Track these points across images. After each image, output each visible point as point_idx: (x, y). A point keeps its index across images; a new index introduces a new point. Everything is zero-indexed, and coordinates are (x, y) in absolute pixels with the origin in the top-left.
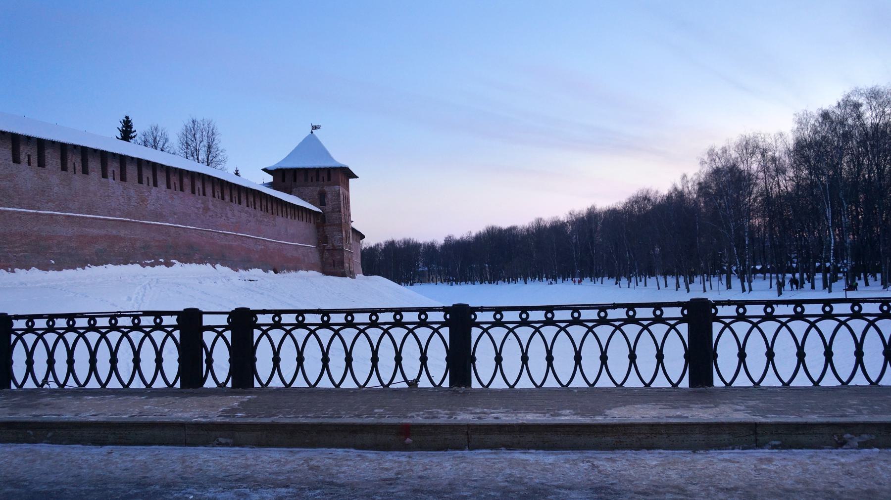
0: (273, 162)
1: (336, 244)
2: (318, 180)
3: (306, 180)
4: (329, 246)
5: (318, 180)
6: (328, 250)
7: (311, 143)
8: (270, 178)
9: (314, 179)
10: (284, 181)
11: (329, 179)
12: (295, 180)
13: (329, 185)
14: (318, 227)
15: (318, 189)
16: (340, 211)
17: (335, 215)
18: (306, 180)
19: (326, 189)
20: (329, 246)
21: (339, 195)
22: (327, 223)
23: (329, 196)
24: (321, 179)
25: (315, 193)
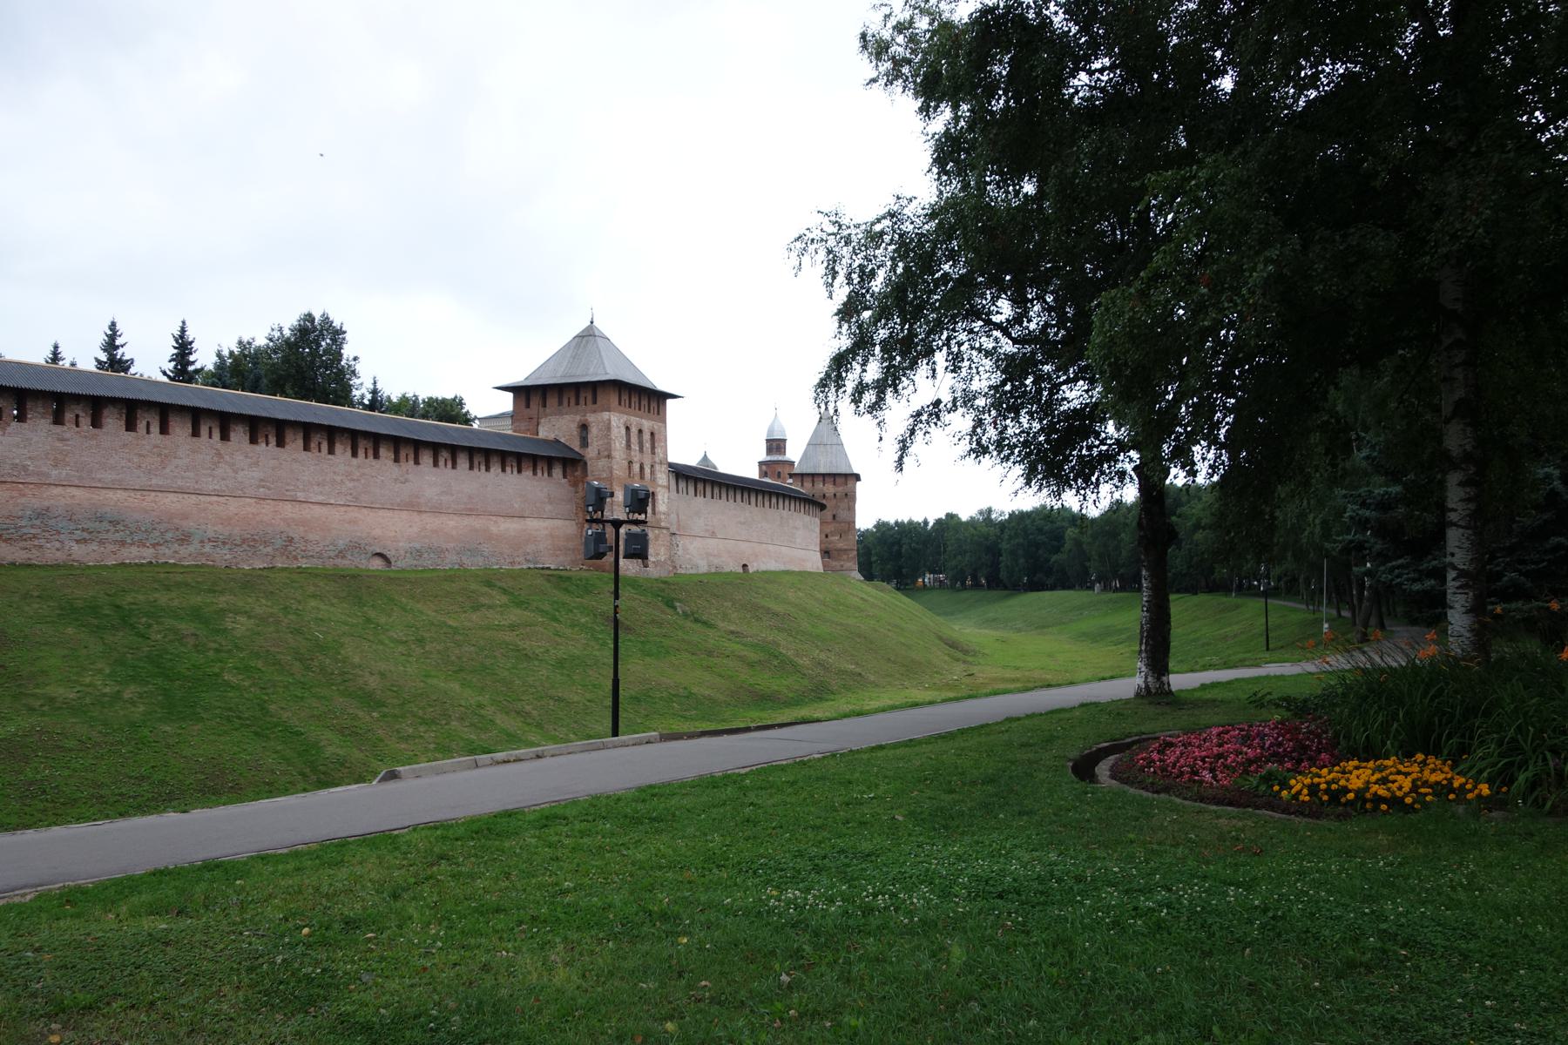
0: (519, 377)
2: (577, 403)
3: (560, 403)
8: (506, 403)
9: (573, 401)
10: (528, 406)
11: (595, 402)
14: (575, 484)
15: (578, 418)
16: (609, 456)
17: (602, 463)
18: (560, 403)
19: (591, 418)
21: (609, 428)
23: (594, 431)
24: (582, 401)
25: (574, 426)
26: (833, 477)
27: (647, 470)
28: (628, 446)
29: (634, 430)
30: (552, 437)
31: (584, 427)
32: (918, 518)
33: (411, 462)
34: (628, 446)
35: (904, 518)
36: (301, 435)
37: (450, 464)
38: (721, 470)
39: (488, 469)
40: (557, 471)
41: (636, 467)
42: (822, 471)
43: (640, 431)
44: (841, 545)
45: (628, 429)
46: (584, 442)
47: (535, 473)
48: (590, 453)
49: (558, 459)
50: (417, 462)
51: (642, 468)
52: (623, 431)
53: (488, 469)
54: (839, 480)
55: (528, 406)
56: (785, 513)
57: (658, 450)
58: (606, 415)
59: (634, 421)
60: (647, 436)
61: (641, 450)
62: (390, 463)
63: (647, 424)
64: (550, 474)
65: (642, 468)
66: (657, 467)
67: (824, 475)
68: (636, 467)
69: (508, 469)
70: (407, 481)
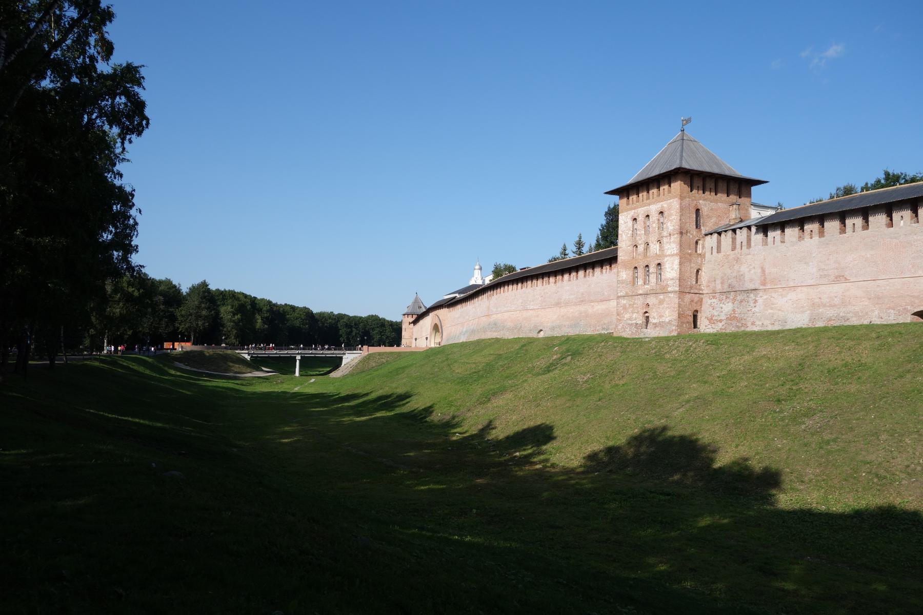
66: (665, 240)
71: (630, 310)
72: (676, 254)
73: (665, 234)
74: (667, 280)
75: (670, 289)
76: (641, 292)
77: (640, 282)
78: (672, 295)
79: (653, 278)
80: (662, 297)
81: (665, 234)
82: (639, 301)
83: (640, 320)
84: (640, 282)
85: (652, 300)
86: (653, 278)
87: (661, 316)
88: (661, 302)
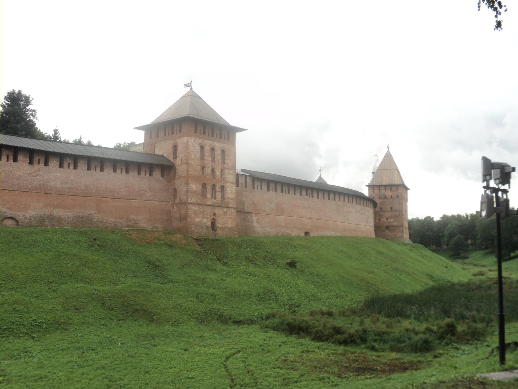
0: (149, 120)
1: (183, 197)
2: (173, 133)
3: (165, 135)
4: (177, 201)
5: (173, 133)
6: (176, 204)
7: (193, 97)
9: (170, 132)
11: (180, 132)
12: (158, 137)
13: (180, 137)
14: (169, 181)
20: (177, 201)
21: (187, 146)
22: (177, 177)
23: (180, 148)
25: (171, 147)
26: (390, 186)
27: (218, 173)
28: (202, 157)
29: (207, 149)
30: (161, 154)
31: (175, 147)
32: (463, 213)
33: (42, 164)
34: (202, 157)
35: (451, 212)
36: (28, 156)
37: (72, 167)
38: (329, 183)
39: (102, 170)
40: (157, 173)
41: (208, 170)
42: (384, 183)
43: (213, 149)
44: (395, 224)
45: (202, 147)
46: (175, 157)
47: (139, 173)
48: (178, 162)
49: (158, 165)
50: (46, 164)
51: (213, 170)
52: (198, 148)
53: (102, 170)
54: (393, 188)
55: (151, 138)
56: (341, 203)
57: (228, 161)
58: (186, 138)
59: (208, 143)
60: (218, 152)
61: (213, 160)
62: (26, 164)
63: (218, 146)
64: (151, 174)
65: (213, 170)
66: (226, 171)
67: (385, 186)
68: (208, 170)
69: (118, 171)
70: (37, 175)
71: (201, 215)
72: (234, 183)
73: (226, 166)
74: (228, 198)
75: (230, 205)
76: (209, 203)
77: (209, 195)
78: (232, 210)
79: (218, 195)
80: (225, 210)
81: (226, 166)
82: (208, 210)
83: (209, 224)
84: (209, 195)
85: (218, 211)
86: (218, 195)
87: (225, 224)
88: (225, 214)
